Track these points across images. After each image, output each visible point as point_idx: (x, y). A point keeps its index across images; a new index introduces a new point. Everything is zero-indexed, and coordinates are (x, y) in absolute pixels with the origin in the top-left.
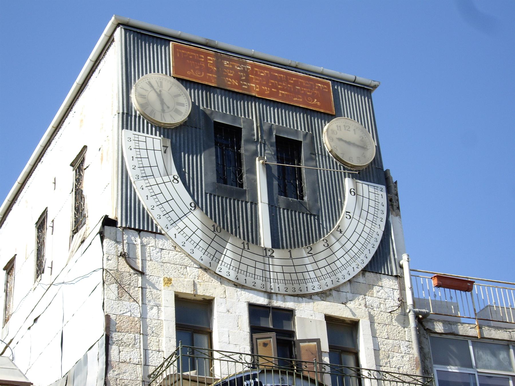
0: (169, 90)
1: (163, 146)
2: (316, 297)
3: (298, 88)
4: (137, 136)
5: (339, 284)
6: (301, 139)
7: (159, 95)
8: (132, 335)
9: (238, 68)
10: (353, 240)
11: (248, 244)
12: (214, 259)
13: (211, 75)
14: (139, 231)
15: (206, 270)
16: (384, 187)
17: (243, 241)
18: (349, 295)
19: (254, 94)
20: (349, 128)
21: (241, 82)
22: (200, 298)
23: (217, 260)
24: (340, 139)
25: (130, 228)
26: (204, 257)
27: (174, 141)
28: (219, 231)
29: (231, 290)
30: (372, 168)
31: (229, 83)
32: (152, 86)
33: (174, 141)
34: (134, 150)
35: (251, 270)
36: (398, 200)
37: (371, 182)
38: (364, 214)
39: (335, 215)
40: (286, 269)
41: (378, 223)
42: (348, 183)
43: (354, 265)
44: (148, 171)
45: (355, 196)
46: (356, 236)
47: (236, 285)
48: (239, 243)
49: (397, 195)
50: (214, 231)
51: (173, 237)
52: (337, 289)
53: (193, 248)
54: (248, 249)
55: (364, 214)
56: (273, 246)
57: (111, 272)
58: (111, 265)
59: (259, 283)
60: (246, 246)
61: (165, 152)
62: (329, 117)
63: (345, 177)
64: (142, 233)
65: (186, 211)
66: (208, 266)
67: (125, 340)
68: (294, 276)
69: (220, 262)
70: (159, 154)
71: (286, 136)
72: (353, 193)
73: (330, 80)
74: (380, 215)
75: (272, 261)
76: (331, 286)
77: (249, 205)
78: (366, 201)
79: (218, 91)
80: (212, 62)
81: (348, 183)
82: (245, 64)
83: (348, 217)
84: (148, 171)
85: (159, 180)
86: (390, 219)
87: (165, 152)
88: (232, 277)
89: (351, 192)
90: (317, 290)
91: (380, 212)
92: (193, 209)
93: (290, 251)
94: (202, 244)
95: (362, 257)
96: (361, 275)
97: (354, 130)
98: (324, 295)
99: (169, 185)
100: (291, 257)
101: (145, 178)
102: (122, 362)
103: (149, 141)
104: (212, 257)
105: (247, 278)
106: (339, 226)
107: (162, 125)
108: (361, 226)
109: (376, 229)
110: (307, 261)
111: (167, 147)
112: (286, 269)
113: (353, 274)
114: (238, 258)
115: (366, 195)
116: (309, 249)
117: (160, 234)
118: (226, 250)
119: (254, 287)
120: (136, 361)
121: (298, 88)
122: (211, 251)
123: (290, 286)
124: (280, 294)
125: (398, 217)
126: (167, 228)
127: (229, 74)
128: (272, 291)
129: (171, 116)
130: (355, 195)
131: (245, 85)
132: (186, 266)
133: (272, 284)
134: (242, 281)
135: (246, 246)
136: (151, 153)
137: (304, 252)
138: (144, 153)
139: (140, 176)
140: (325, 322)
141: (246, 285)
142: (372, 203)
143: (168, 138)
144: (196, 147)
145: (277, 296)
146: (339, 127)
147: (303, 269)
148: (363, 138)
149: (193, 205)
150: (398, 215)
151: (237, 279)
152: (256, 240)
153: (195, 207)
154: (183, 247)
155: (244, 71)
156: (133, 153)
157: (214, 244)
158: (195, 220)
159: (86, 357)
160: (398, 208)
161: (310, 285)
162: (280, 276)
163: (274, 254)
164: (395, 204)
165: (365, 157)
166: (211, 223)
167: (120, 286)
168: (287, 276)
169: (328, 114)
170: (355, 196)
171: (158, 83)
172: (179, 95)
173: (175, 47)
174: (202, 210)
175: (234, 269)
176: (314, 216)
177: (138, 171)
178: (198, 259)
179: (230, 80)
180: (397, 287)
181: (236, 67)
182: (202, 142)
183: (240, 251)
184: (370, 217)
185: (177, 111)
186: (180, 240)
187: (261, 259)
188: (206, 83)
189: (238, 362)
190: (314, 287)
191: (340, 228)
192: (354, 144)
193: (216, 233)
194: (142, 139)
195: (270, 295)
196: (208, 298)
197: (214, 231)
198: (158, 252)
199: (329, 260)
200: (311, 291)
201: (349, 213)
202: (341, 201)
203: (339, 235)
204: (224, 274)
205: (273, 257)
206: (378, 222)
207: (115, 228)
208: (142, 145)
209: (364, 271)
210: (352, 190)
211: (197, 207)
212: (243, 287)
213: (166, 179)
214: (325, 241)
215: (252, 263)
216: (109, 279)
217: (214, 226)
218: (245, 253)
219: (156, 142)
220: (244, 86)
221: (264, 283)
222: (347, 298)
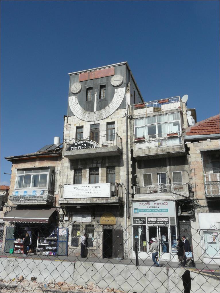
7: (76, 87)
15: (83, 120)
18: (113, 116)
24: (114, 81)
39: (111, 100)
48: (89, 112)
55: (119, 96)
79: (88, 81)
81: (116, 90)
108: (117, 99)
137: (103, 110)
166: (83, 110)
185: (79, 89)
187: (93, 115)
190: (104, 117)
192: (118, 80)
205: (96, 113)
206: (122, 97)
209: (117, 109)
213: (76, 104)
218: (90, 114)
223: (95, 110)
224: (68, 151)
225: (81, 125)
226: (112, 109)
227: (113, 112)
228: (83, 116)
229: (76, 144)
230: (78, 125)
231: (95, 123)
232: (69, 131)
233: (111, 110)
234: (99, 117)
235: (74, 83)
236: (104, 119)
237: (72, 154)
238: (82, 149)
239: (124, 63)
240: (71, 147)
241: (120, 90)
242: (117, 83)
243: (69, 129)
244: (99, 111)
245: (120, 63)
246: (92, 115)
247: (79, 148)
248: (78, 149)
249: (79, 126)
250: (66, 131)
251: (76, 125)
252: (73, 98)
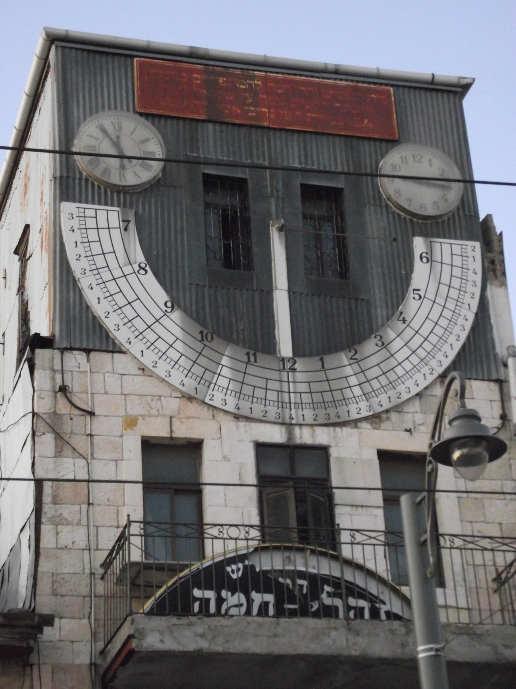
0: (132, 134)
1: (123, 221)
2: (365, 425)
3: (337, 105)
4: (82, 210)
5: (400, 401)
6: (340, 185)
8: (77, 508)
9: (242, 87)
10: (425, 331)
11: (254, 354)
12: (203, 381)
13: (198, 102)
14: (88, 351)
15: (190, 398)
16: (477, 245)
17: (246, 351)
19: (266, 124)
20: (422, 157)
21: (246, 108)
22: (184, 442)
23: (207, 384)
25: (72, 349)
26: (186, 381)
27: (140, 211)
28: (209, 338)
29: (228, 424)
30: (459, 215)
31: (227, 111)
32: (104, 131)
33: (140, 211)
34: (77, 232)
35: (260, 393)
36: (503, 261)
37: (456, 238)
40: (315, 387)
42: (419, 244)
43: (426, 370)
44: (100, 261)
45: (429, 264)
46: (429, 325)
47: (237, 417)
49: (502, 253)
50: (202, 340)
51: (138, 355)
52: (398, 408)
53: (169, 368)
54: (256, 361)
55: (443, 289)
57: (44, 416)
58: (44, 406)
59: (272, 412)
60: (252, 359)
61: (126, 229)
62: (393, 142)
63: (414, 236)
64: (92, 354)
65: (158, 314)
66: (192, 393)
67: (65, 515)
68: (328, 397)
69: (212, 386)
70: (116, 234)
71: (317, 183)
72: (425, 260)
73: (392, 85)
74: (470, 288)
75: (294, 377)
76: (386, 405)
77: (257, 294)
78: (447, 269)
79: (210, 126)
80: (199, 82)
81: (419, 244)
82: (253, 77)
83: (417, 297)
84: (100, 261)
85: (117, 273)
86: (489, 293)
87: (126, 229)
88: (230, 407)
89: (421, 258)
90: (364, 413)
91: (470, 284)
92: (169, 310)
93: (322, 360)
94: (183, 361)
95: (439, 356)
96: (438, 384)
97: (430, 160)
98: (375, 419)
99: (132, 278)
100: (323, 366)
101: (96, 272)
102: (61, 548)
103: (102, 215)
104: (198, 379)
105: (254, 406)
106: (401, 313)
107: (121, 188)
108: (437, 309)
109: (463, 312)
110: (349, 371)
111: (129, 221)
112: (315, 387)
113: (423, 384)
114: (240, 377)
115: (447, 259)
116: (353, 352)
117: (120, 352)
118: (220, 366)
119: (264, 419)
120: (83, 544)
121: (337, 105)
122: (198, 370)
123: (322, 413)
124: (307, 425)
125: (503, 288)
126: (130, 343)
127: (227, 98)
128: (294, 422)
129: (135, 173)
130: (428, 261)
131: (252, 111)
132: (160, 396)
133: (293, 411)
134: (246, 412)
135: (252, 359)
136: (104, 234)
137: (344, 358)
138: (93, 235)
139: (88, 269)
140: (377, 461)
141: (251, 416)
142: (457, 272)
143: (131, 207)
144: (175, 216)
145: (300, 428)
146: (404, 159)
147: (343, 383)
148: (444, 171)
149: (169, 304)
150: (503, 284)
151: (238, 409)
152: (270, 346)
153: (173, 307)
154: (154, 369)
155: (250, 88)
156: (77, 236)
157: (202, 360)
158: (173, 326)
159: (19, 540)
160: (504, 274)
161: (353, 408)
162: (306, 398)
163: (296, 366)
164: (498, 268)
165: (446, 200)
166: (196, 329)
167: (58, 437)
168: (317, 397)
169: (387, 141)
170: (429, 264)
171: (114, 126)
172: (148, 140)
173: (140, 64)
174: (185, 311)
175: (233, 394)
176: (363, 300)
177: (84, 263)
178: (176, 383)
179: (229, 106)
180: (497, 396)
181: (238, 85)
182: (184, 207)
183: (242, 367)
184: (454, 294)
186: (148, 360)
187: (275, 375)
188: (191, 116)
189: (216, 538)
190: (360, 408)
191: (402, 316)
193: (206, 342)
194: (92, 213)
195: (289, 426)
196: (194, 441)
197: (202, 340)
198: (117, 379)
199: (385, 367)
200: (354, 416)
201: (419, 290)
202: (406, 273)
203: (402, 326)
204: (217, 402)
206: (467, 299)
207: (51, 350)
208: (91, 223)
210: (424, 255)
211: (176, 307)
212: (248, 419)
213: (128, 270)
214: (378, 338)
215: (262, 383)
216: (41, 427)
217: (201, 333)
218: (251, 369)
219: (111, 216)
220: (250, 114)
221: (280, 411)
222: (414, 422)
223: (285, 347)
224: (174, 620)
225: (183, 431)
226: (407, 365)
227: (415, 390)
228: (198, 370)
229: (235, 572)
230: (158, 429)
231: (290, 435)
232: (81, 463)
233: (399, 371)
234: (317, 397)
235: (93, 111)
236: (355, 423)
237: (220, 649)
238: (293, 613)
240: (197, 593)
241: (446, 248)
242: (426, 200)
243: (80, 443)
244: (314, 363)
246: (268, 374)
247: (264, 606)
248: (248, 612)
249: (164, 433)
250: (58, 453)
251: (140, 422)
252: (103, 223)
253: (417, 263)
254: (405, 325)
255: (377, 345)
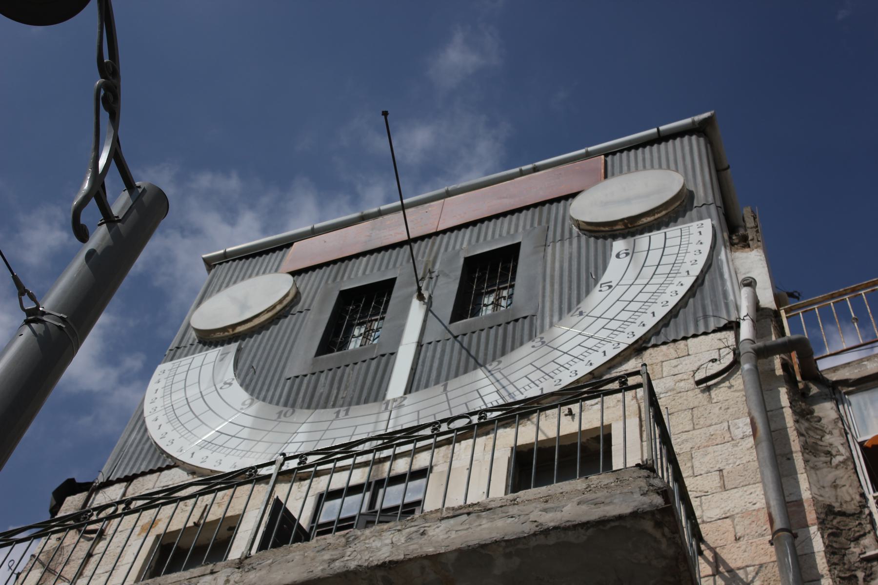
10: (610, 314)
38: (648, 271)
41: (683, 271)
55: (648, 271)
56: (408, 390)
60: (342, 413)
61: (222, 360)
87: (222, 360)
111: (228, 353)
137: (480, 373)
187: (373, 418)
203: (576, 319)
205: (400, 407)
218: (337, 424)
239: (688, 120)
245: (655, 130)
253: (613, 262)
254: (582, 317)
255: (533, 347)
